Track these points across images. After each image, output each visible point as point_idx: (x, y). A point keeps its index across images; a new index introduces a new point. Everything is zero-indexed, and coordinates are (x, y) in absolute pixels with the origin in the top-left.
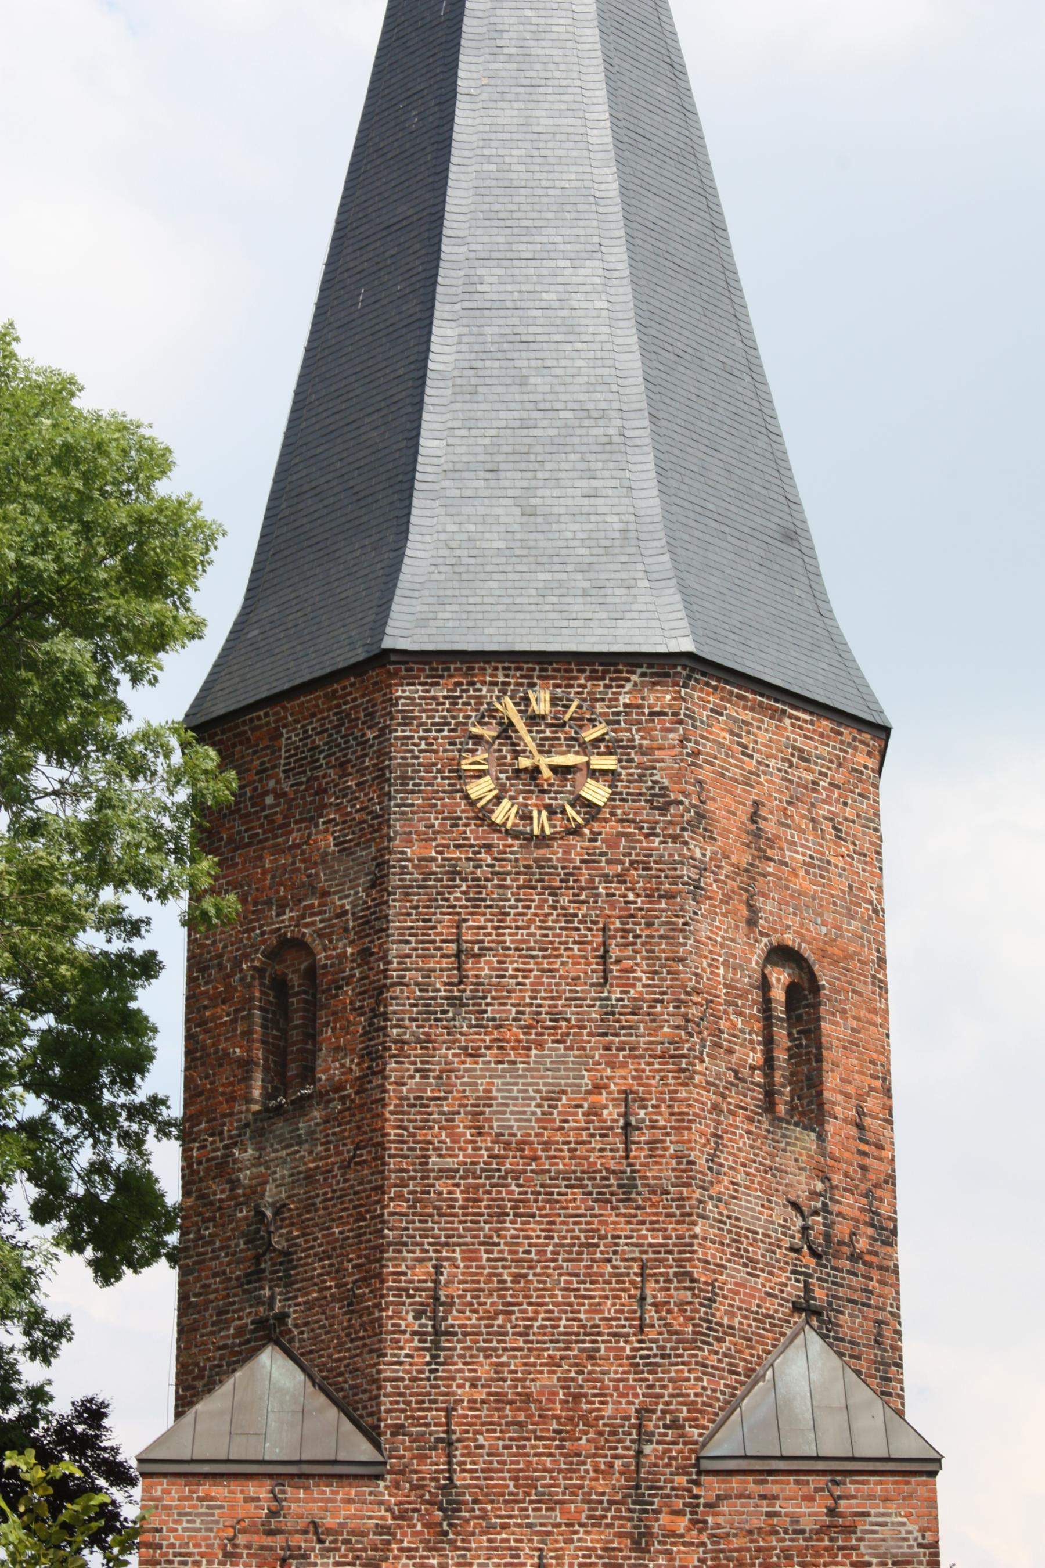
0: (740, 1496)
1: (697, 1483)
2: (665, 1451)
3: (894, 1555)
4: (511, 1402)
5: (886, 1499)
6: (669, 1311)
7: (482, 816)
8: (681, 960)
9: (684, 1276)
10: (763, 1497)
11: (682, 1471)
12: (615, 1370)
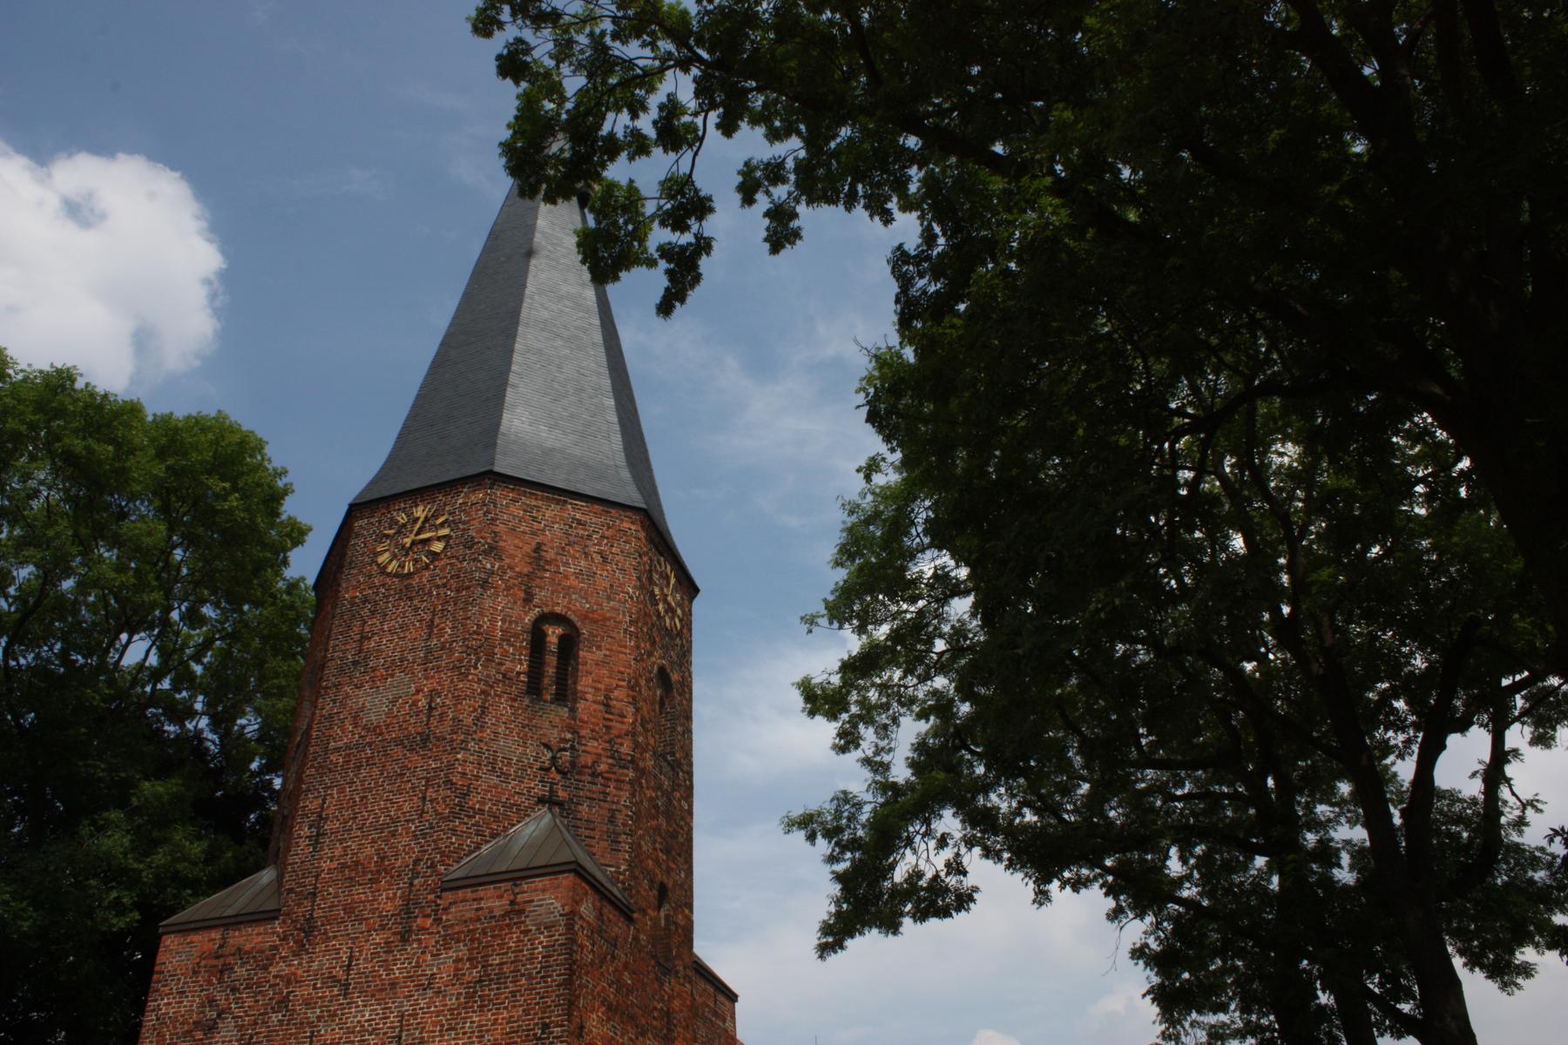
0: (462, 901)
1: (440, 897)
2: (425, 881)
3: (545, 923)
4: (350, 866)
5: (544, 890)
7: (382, 569)
8: (469, 618)
10: (474, 900)
11: (433, 891)
12: (405, 840)
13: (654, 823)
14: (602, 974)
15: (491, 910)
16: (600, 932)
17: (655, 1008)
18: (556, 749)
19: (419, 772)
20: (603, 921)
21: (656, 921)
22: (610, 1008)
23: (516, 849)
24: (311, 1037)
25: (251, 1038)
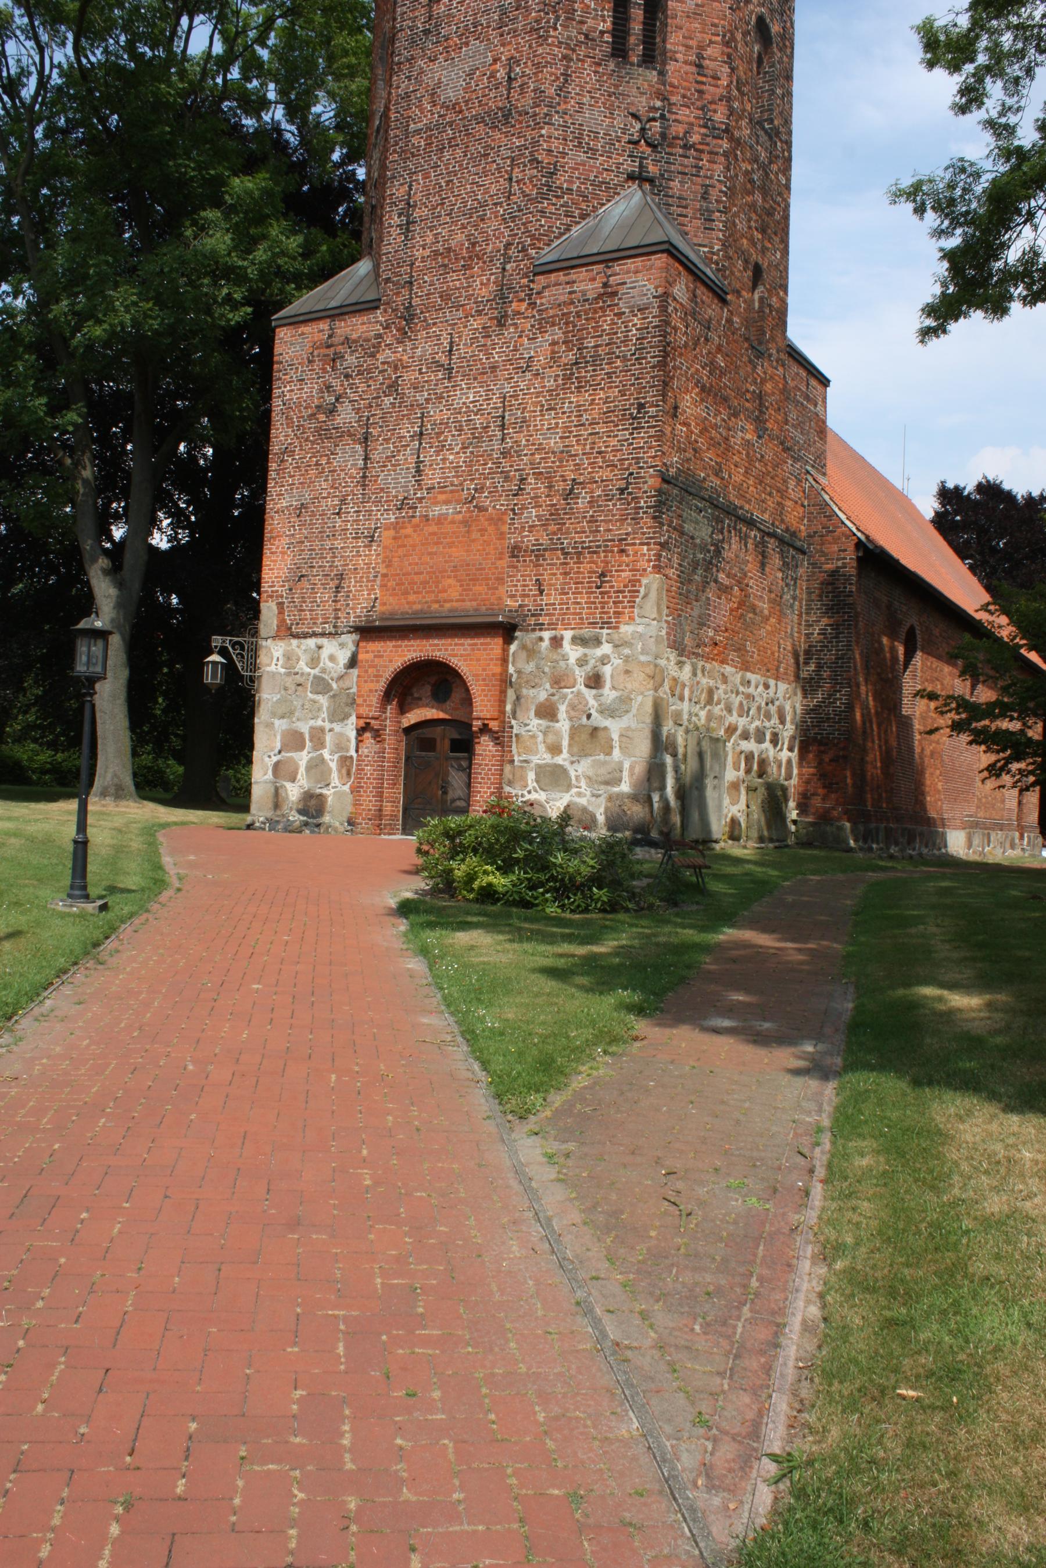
0: (554, 286)
1: (532, 281)
2: (517, 266)
4: (441, 254)
5: (636, 272)
6: (524, 184)
9: (534, 161)
10: (567, 283)
13: (749, 199)
14: (695, 356)
15: (584, 293)
16: (694, 314)
17: (748, 391)
18: (645, 119)
19: (504, 152)
20: (696, 303)
21: (749, 303)
22: (703, 389)
23: (606, 231)
24: (422, 418)
25: (368, 419)
